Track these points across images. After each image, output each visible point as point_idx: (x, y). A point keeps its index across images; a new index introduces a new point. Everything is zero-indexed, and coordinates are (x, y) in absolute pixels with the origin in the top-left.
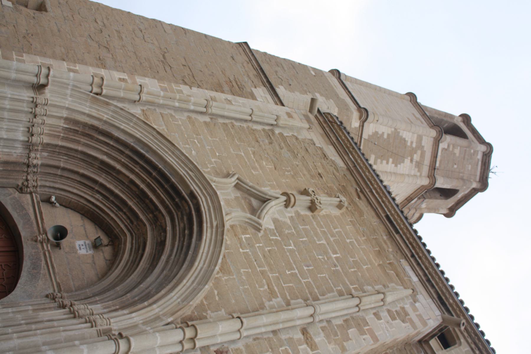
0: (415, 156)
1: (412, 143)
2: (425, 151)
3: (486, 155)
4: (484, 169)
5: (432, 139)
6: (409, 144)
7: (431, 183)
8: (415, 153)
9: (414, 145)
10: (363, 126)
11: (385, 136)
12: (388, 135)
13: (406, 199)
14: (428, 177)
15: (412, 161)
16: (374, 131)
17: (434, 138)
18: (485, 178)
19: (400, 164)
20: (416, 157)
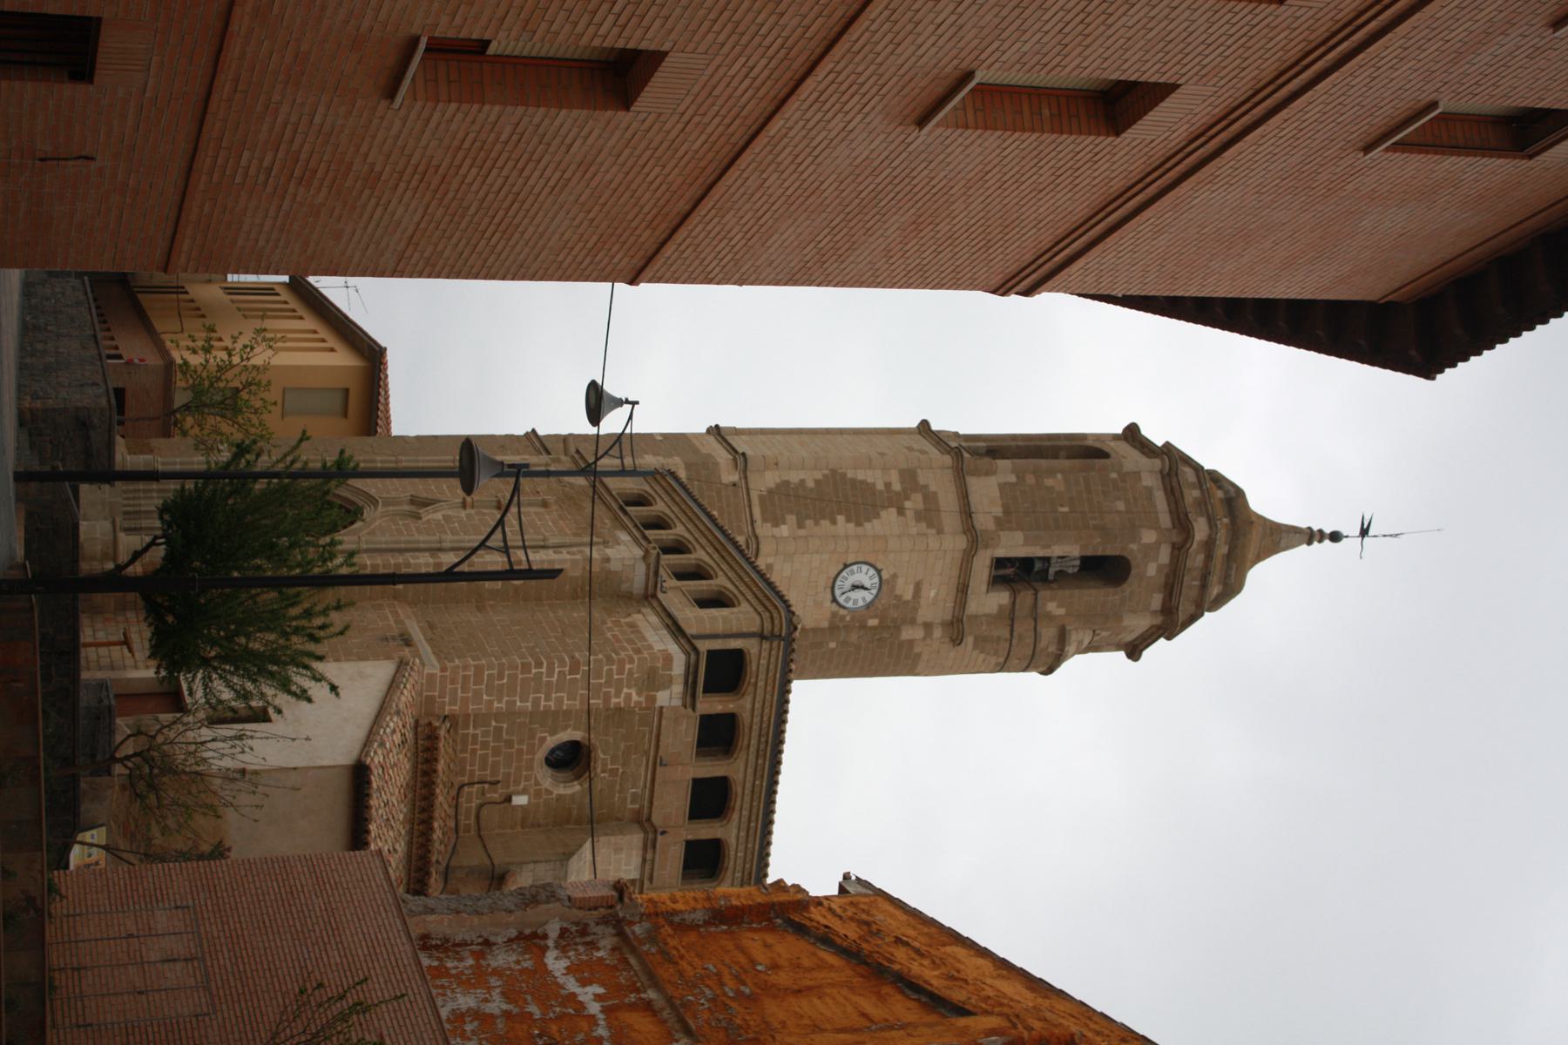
0: (908, 504)
1: (888, 485)
2: (935, 493)
3: (1168, 474)
4: (1176, 502)
5: (950, 471)
6: (880, 486)
7: (970, 539)
8: (907, 498)
9: (897, 487)
10: (746, 478)
11: (810, 484)
12: (817, 482)
13: (958, 591)
14: (965, 533)
15: (901, 511)
16: (778, 481)
17: (952, 467)
18: (1182, 516)
19: (869, 520)
20: (914, 503)
